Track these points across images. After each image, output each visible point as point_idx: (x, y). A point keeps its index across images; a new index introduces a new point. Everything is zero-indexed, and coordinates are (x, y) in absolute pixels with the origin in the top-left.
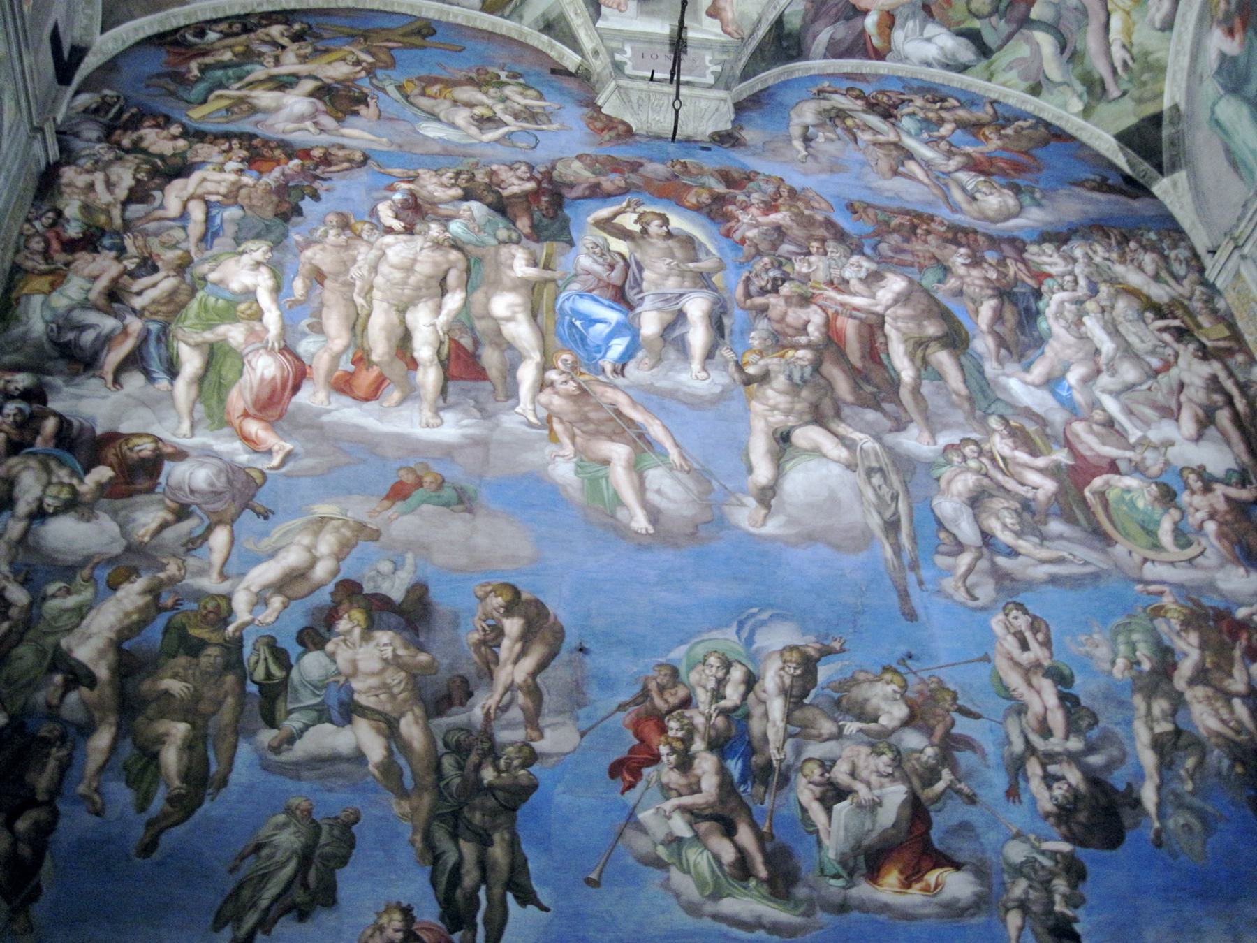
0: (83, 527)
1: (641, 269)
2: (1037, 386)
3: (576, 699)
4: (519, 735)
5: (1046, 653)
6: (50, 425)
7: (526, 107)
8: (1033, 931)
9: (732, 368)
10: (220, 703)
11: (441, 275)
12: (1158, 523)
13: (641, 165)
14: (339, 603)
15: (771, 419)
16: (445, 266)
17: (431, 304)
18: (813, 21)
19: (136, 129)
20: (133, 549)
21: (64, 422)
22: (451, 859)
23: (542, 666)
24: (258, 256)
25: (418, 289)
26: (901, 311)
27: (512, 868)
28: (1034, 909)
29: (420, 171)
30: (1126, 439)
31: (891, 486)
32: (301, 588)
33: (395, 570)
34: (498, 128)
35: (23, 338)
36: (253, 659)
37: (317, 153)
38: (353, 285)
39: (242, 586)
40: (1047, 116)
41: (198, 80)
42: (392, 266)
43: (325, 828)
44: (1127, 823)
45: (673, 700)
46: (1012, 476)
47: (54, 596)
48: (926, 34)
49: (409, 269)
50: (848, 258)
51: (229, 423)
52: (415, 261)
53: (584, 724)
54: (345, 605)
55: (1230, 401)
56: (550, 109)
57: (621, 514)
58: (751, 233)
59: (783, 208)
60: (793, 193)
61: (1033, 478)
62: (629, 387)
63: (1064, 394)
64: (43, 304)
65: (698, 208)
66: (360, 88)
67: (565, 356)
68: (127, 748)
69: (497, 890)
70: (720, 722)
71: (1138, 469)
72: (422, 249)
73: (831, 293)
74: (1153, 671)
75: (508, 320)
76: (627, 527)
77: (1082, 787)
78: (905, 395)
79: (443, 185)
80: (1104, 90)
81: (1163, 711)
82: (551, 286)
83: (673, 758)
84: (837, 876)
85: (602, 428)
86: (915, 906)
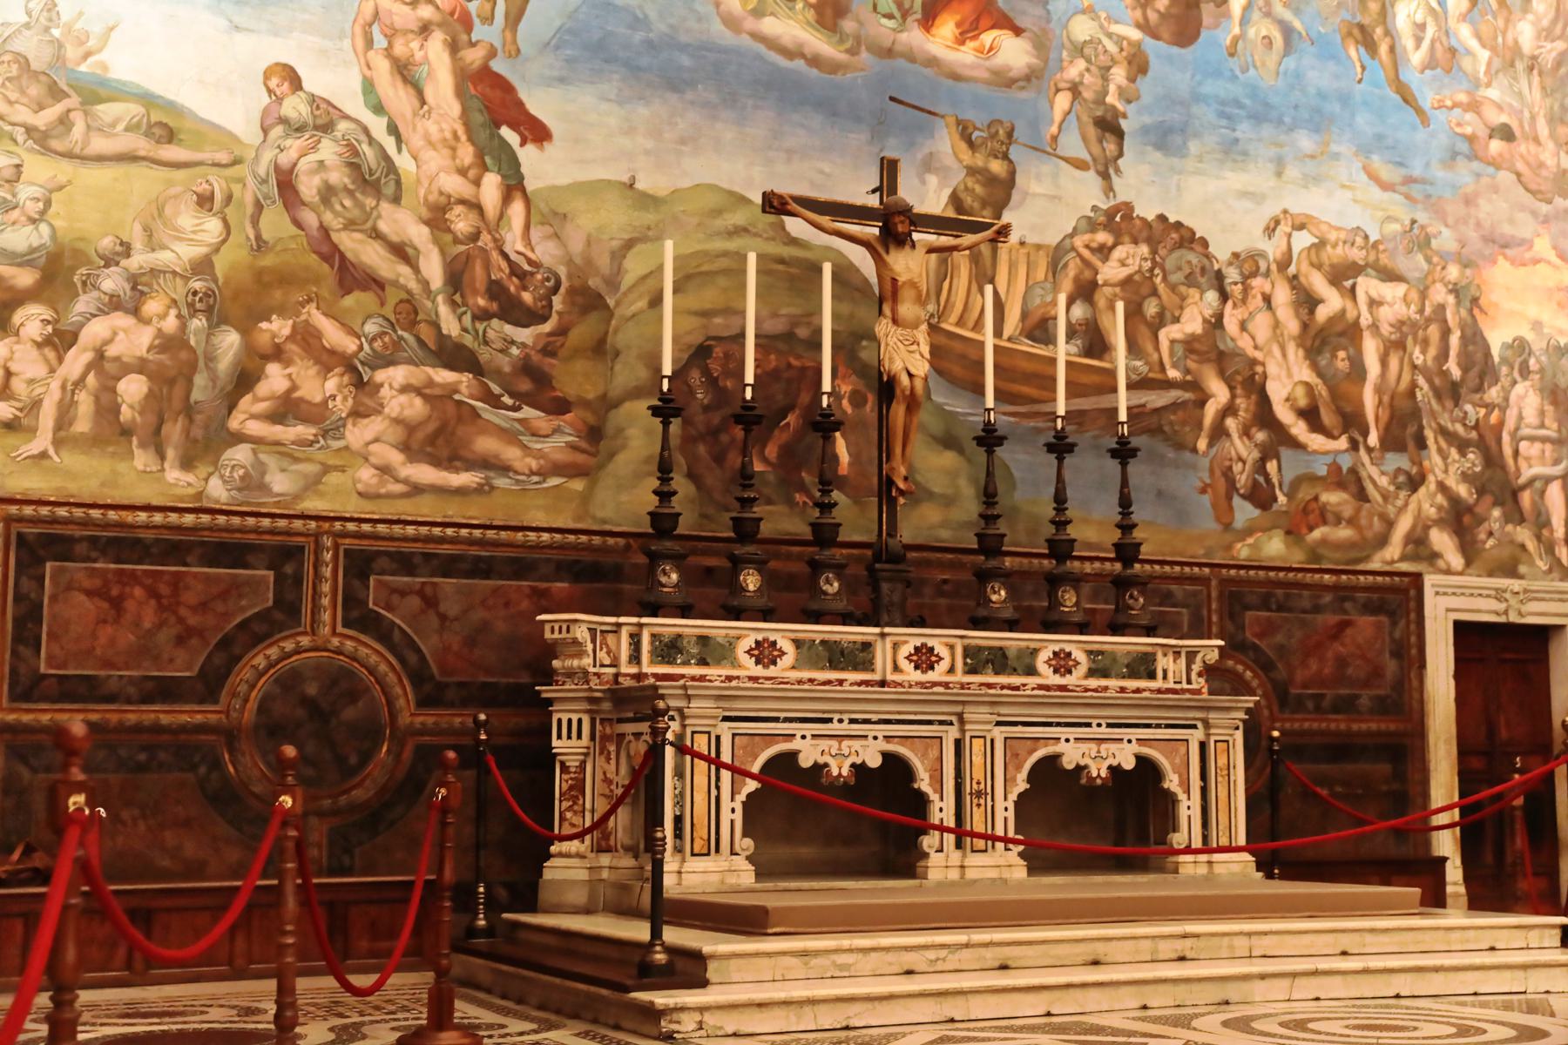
8: (1078, 118)
28: (1088, 94)
44: (1207, 20)
84: (890, 16)
86: (965, 66)
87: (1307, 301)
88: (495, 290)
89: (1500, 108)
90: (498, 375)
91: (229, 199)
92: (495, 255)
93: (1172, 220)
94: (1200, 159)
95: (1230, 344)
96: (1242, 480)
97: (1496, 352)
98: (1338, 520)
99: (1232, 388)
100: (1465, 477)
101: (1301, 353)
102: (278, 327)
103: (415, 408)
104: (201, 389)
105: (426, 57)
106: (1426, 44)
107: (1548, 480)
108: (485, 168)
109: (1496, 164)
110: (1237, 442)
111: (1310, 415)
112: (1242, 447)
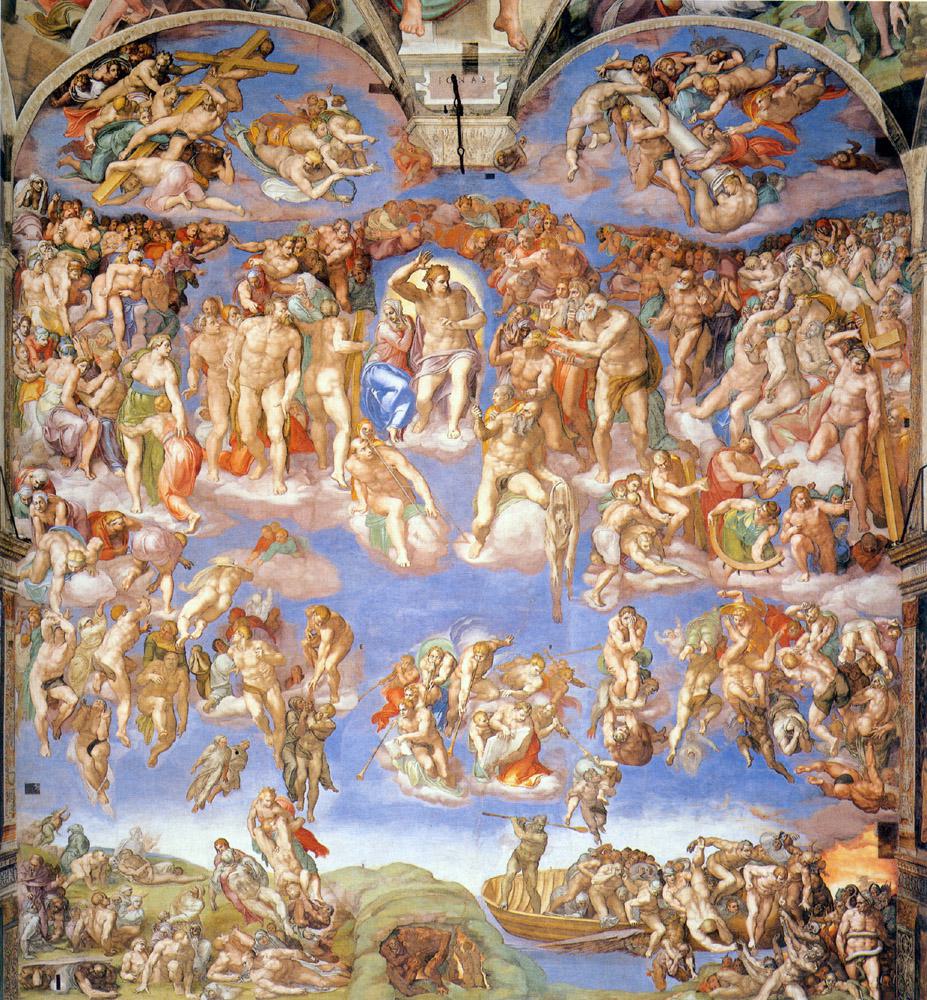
1: (423, 333)
4: (327, 699)
5: (639, 643)
6: (60, 508)
7: (347, 145)
9: (476, 426)
11: (284, 356)
12: (755, 539)
13: (435, 208)
15: (497, 469)
16: (287, 347)
17: (278, 386)
19: (61, 221)
21: (67, 506)
23: (340, 659)
24: (163, 350)
25: (268, 372)
26: (614, 353)
28: (586, 797)
29: (267, 242)
32: (211, 615)
34: (325, 178)
35: (32, 440)
37: (191, 232)
40: (827, 62)
41: (96, 151)
42: (251, 350)
45: (410, 678)
49: (262, 353)
50: (585, 297)
51: (162, 500)
52: (266, 343)
54: (236, 624)
55: (865, 420)
57: (392, 554)
58: (512, 280)
59: (543, 245)
60: (555, 222)
62: (405, 449)
65: (473, 257)
67: (366, 425)
68: (137, 713)
69: (314, 782)
70: (434, 690)
71: (757, 491)
73: (563, 340)
75: (329, 395)
78: (597, 435)
79: (284, 257)
80: (879, 47)
81: (704, 683)
82: (358, 358)
85: (386, 487)
87: (712, 880)
88: (307, 915)
89: (842, 766)
92: (307, 903)
94: (650, 819)
96: (672, 969)
98: (729, 984)
101: (708, 906)
102: (224, 938)
103: (277, 964)
106: (793, 741)
107: (866, 957)
109: (839, 797)
110: (670, 952)
111: (714, 935)
112: (672, 954)
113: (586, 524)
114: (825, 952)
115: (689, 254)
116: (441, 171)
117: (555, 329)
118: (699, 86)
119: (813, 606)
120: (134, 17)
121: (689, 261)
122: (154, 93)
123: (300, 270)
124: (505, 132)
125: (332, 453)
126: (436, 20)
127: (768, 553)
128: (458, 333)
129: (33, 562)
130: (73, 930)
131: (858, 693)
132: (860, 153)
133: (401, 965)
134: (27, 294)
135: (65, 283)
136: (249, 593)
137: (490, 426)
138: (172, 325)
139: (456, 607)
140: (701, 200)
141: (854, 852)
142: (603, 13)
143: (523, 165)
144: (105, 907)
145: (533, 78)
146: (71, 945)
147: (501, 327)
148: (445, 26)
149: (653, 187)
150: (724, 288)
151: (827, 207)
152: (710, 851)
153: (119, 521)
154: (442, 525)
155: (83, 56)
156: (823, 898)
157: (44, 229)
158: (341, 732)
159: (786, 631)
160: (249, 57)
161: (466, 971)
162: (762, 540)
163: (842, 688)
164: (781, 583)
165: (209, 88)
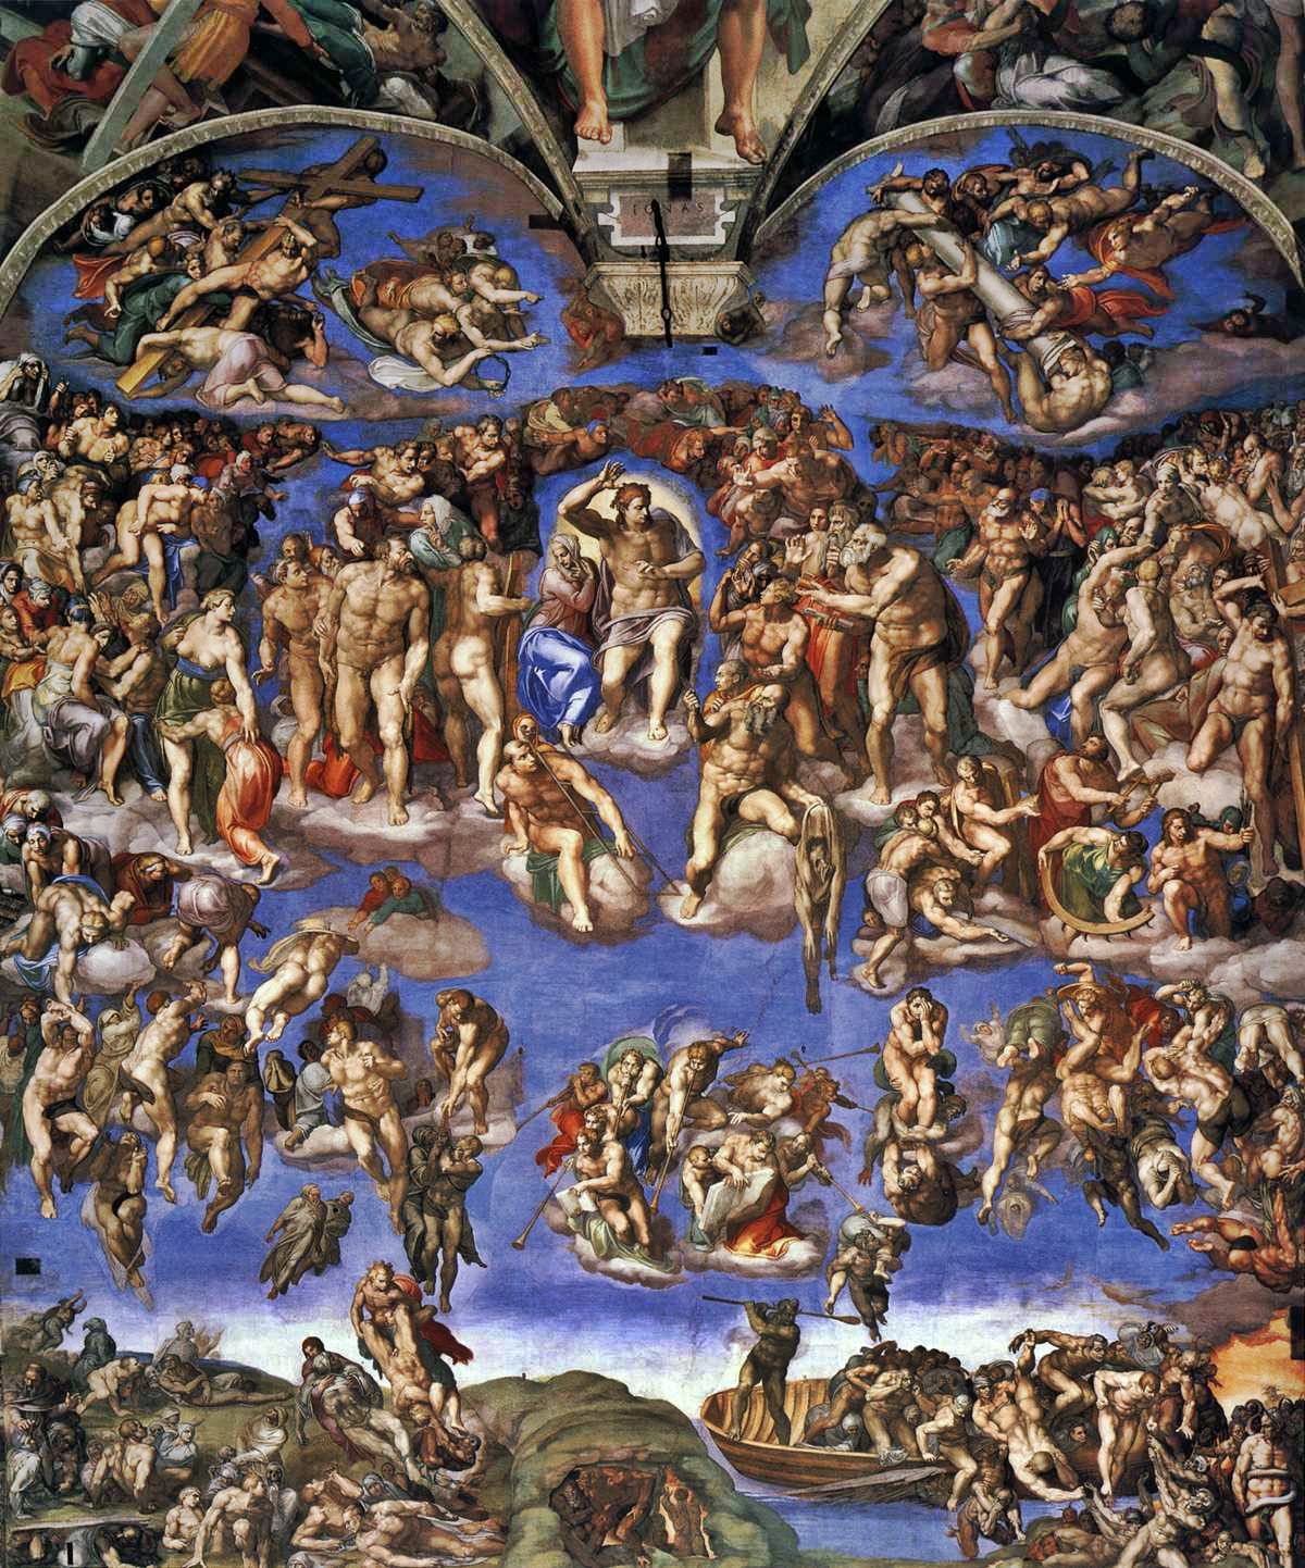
0: (118, 954)
1: (611, 584)
2: (1030, 709)
3: (515, 1097)
4: (469, 1129)
5: (937, 1042)
6: (70, 848)
7: (498, 306)
9: (691, 720)
10: (248, 1110)
12: (1109, 888)
13: (628, 398)
14: (329, 1018)
15: (722, 785)
16: (407, 606)
17: (394, 663)
18: (874, 88)
20: (164, 974)
21: (82, 847)
22: (419, 1229)
23: (489, 1068)
25: (381, 643)
26: (898, 612)
27: (462, 1235)
29: (378, 451)
30: (1116, 776)
31: (829, 862)
32: (298, 1005)
33: (372, 982)
34: (463, 355)
36: (267, 1072)
38: (318, 644)
39: (253, 1004)
40: (1217, 178)
42: (353, 612)
43: (330, 1208)
45: (592, 1096)
46: (964, 840)
47: (109, 1023)
48: (1047, 71)
49: (371, 615)
50: (853, 529)
52: (377, 600)
53: (520, 1119)
55: (1271, 709)
56: (524, 307)
57: (565, 911)
60: (808, 417)
61: (986, 837)
62: (584, 757)
63: (1060, 717)
64: (33, 700)
65: (686, 470)
66: (301, 302)
67: (526, 721)
68: (185, 1148)
69: (450, 1253)
70: (629, 1114)
71: (1113, 817)
72: (383, 581)
73: (821, 593)
74: (1039, 1058)
75: (472, 676)
76: (569, 926)
77: (930, 1172)
79: (403, 473)
81: (1034, 1099)
82: (515, 622)
83: (587, 1147)
84: (703, 1243)
88: (440, 1451)
89: (1241, 1224)
90: (444, 1501)
91: (286, 1417)
92: (440, 1431)
93: (929, 1348)
94: (954, 1303)
95: (979, 1432)
96: (986, 1526)
97: (1228, 1414)
98: (1071, 1548)
99: (978, 1462)
100: (1194, 1511)
101: (1041, 1431)
102: (317, 1486)
104: (276, 1524)
105: (395, 1322)
106: (1169, 1185)
107: (1276, 1507)
108: (433, 1381)
109: (1236, 1269)
110: (983, 1499)
111: (1050, 1476)
112: (986, 1504)
113: (856, 865)
114: (1217, 1499)
115: (1009, 463)
116: (637, 344)
117: (808, 578)
118: (1023, 215)
119: (1198, 986)
120: (177, 119)
121: (1010, 474)
122: (207, 232)
123: (426, 492)
124: (732, 287)
125: (476, 764)
126: (629, 120)
127: (1130, 908)
128: (663, 584)
129: (28, 929)
130: (93, 1474)
131: (1264, 1114)
132: (1266, 311)
133: (582, 1525)
134: (19, 533)
135: (77, 515)
136: (350, 976)
137: (711, 721)
138: (236, 574)
139: (662, 991)
140: (1027, 385)
141: (1257, 1349)
142: (880, 105)
143: (760, 334)
144: (139, 1440)
145: (773, 203)
146: (88, 1499)
147: (728, 575)
148: (644, 129)
149: (957, 366)
150: (1061, 516)
151: (1217, 394)
152: (1044, 1350)
153: (158, 867)
154: (639, 870)
155: (103, 179)
156: (1213, 1419)
157: (43, 435)
158: (491, 1179)
159: (1158, 1022)
160: (348, 177)
161: (679, 1532)
162: (1119, 889)
163: (1240, 1108)
164: (1148, 953)
165: (290, 223)
